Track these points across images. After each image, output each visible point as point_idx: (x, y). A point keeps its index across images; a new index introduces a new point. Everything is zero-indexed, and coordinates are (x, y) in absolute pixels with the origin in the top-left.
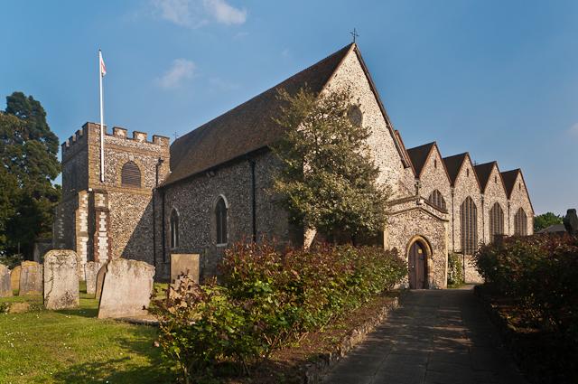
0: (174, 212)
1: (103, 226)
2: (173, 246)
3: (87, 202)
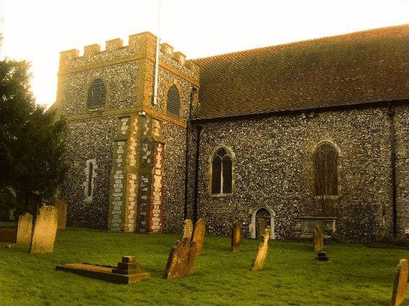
0: (222, 151)
1: (159, 162)
2: (216, 189)
3: (136, 128)
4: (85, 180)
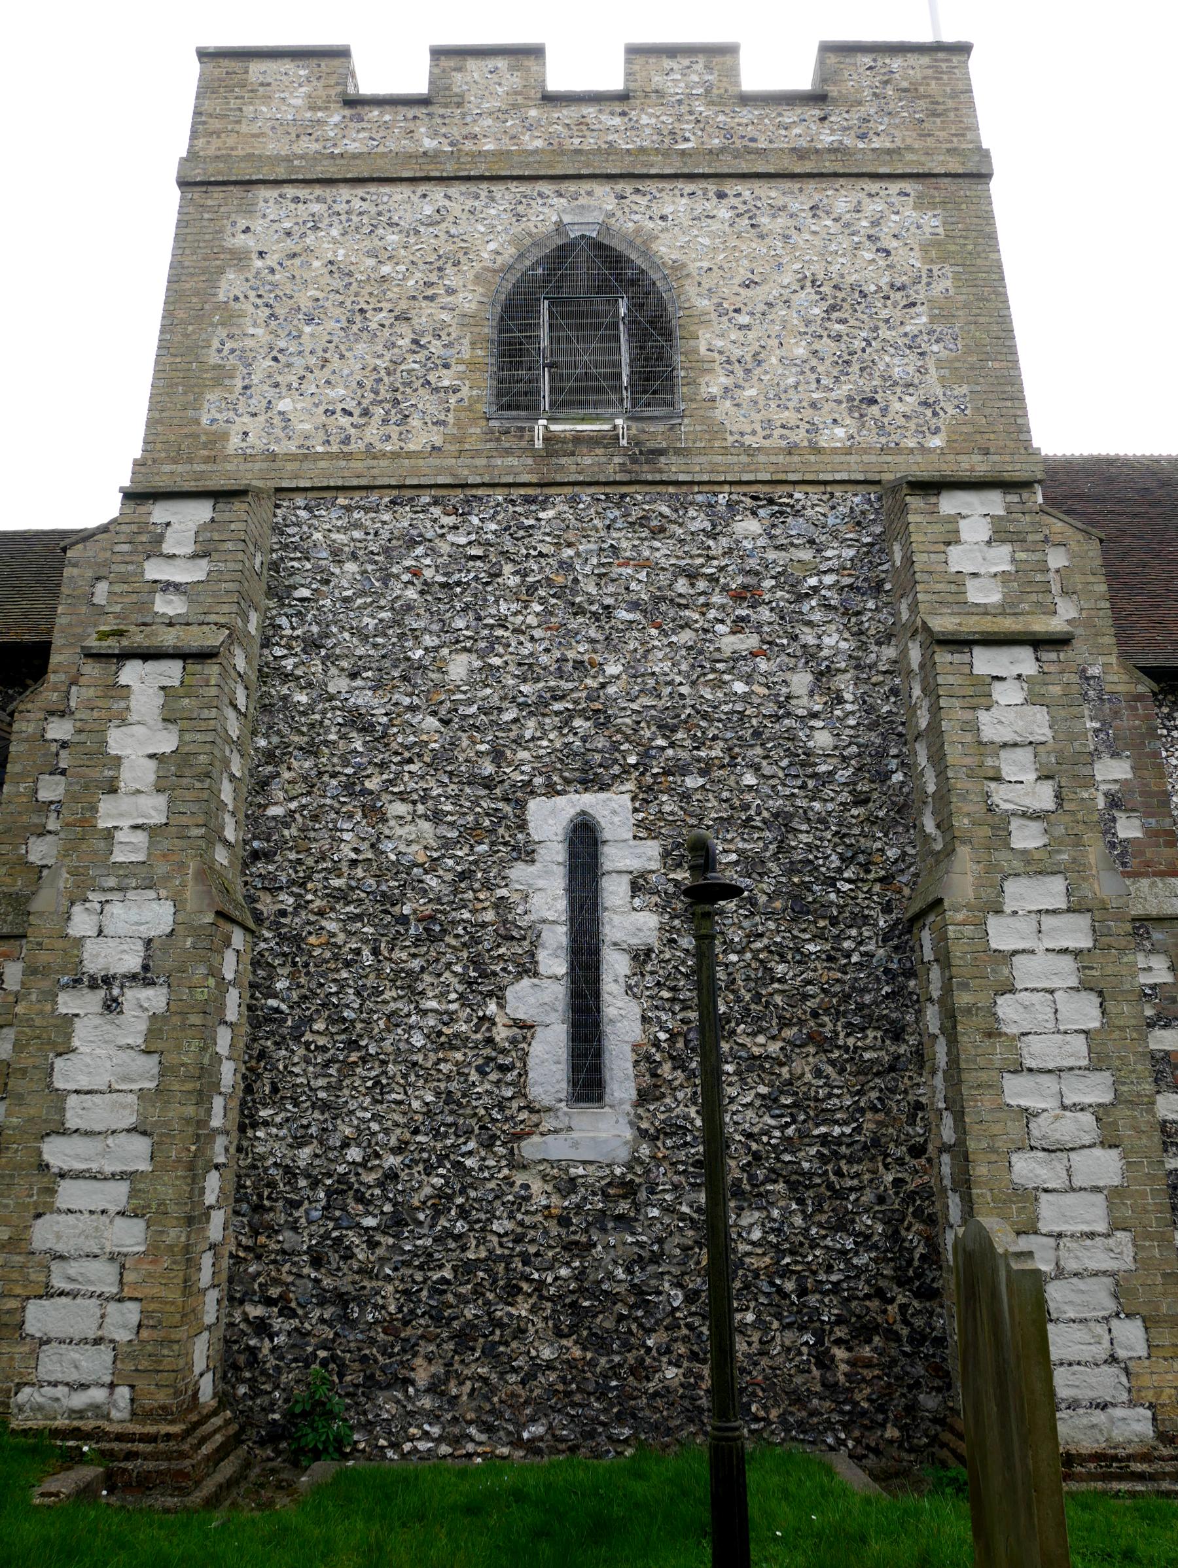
4: (528, 969)
